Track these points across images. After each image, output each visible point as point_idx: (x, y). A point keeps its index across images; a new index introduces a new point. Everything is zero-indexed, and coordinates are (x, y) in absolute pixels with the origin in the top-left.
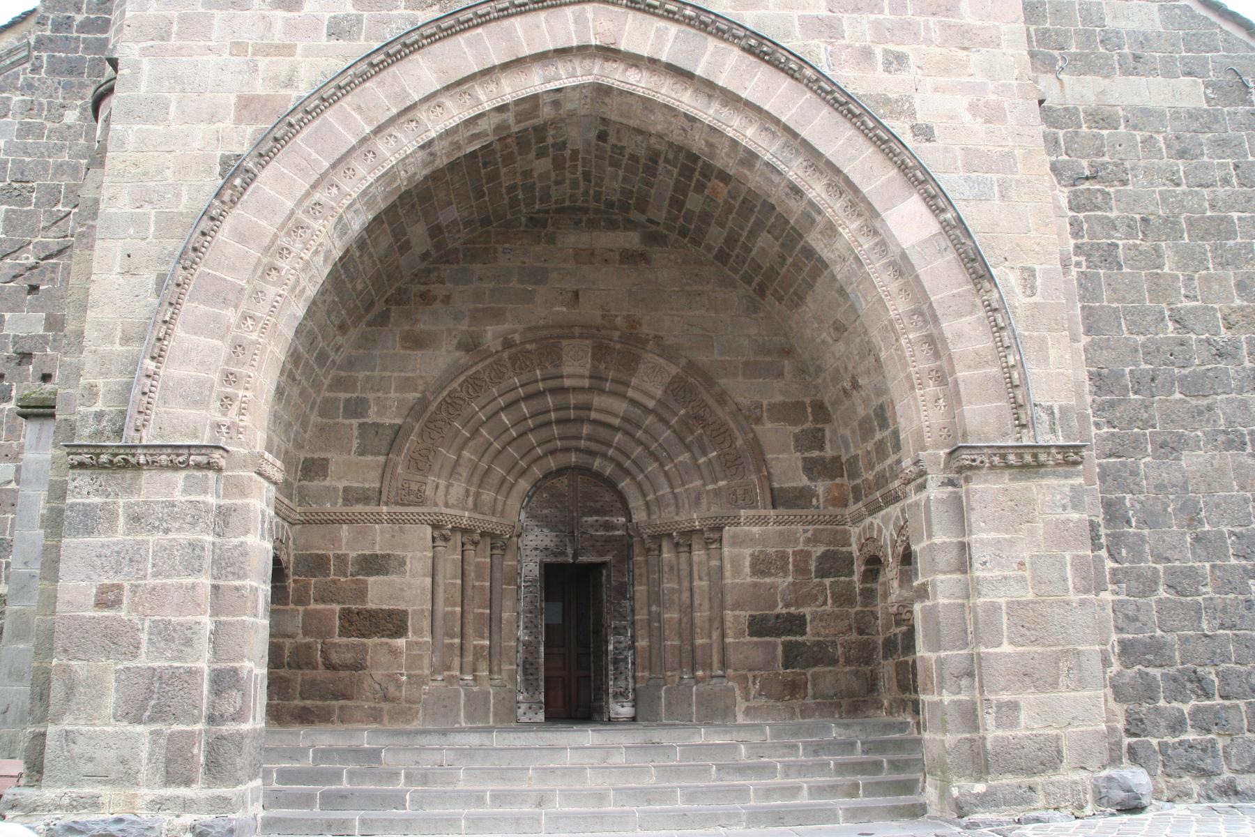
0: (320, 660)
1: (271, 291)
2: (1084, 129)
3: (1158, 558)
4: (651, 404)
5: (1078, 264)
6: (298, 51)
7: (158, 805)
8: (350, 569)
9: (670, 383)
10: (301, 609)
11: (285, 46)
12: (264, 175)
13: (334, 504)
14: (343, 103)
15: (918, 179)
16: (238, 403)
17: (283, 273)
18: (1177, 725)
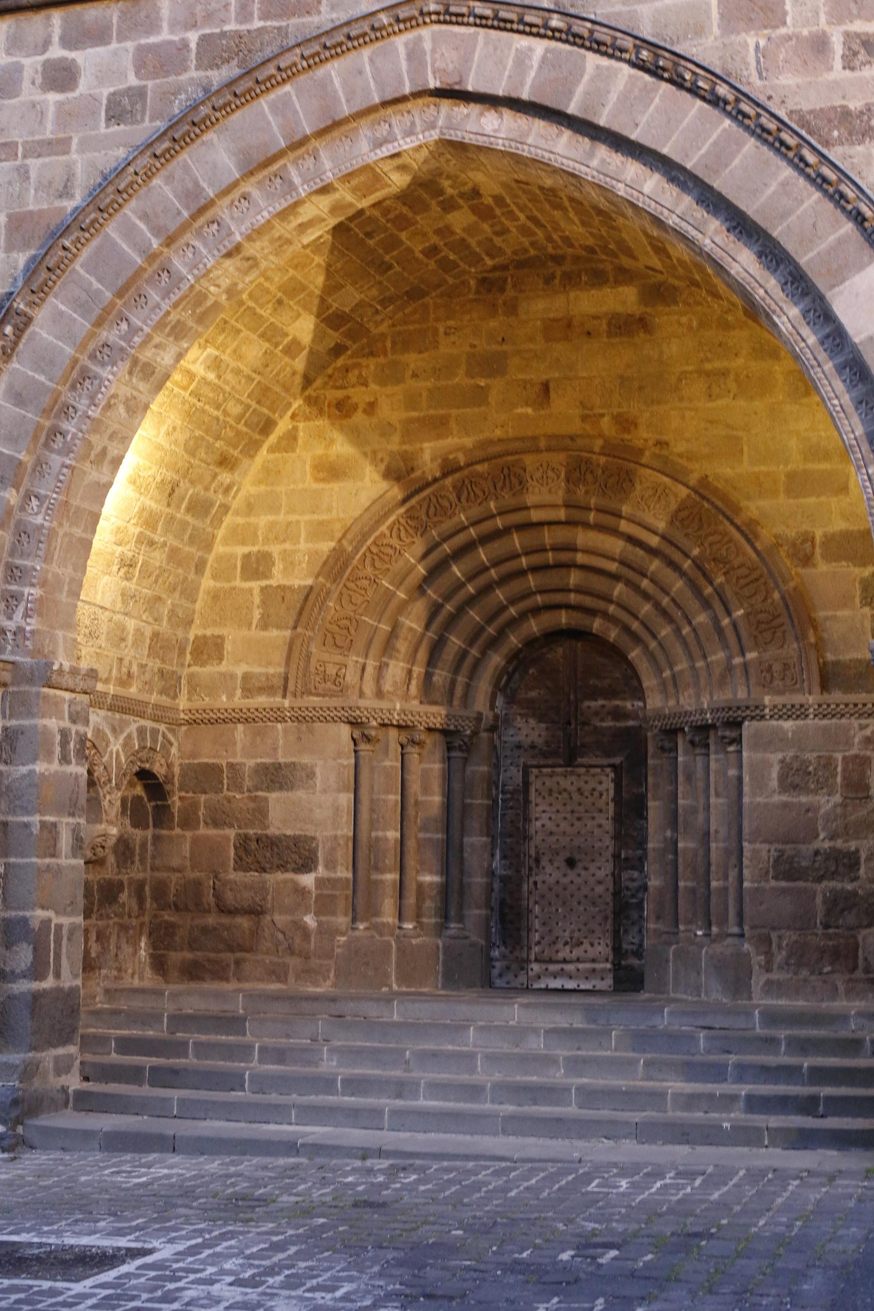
0: (212, 900)
1: (56, 460)
4: (654, 541)
6: (74, 145)
8: (247, 783)
9: (679, 510)
10: (189, 834)
11: (59, 141)
12: (41, 315)
13: (231, 696)
14: (127, 211)
16: (23, 604)
17: (69, 438)
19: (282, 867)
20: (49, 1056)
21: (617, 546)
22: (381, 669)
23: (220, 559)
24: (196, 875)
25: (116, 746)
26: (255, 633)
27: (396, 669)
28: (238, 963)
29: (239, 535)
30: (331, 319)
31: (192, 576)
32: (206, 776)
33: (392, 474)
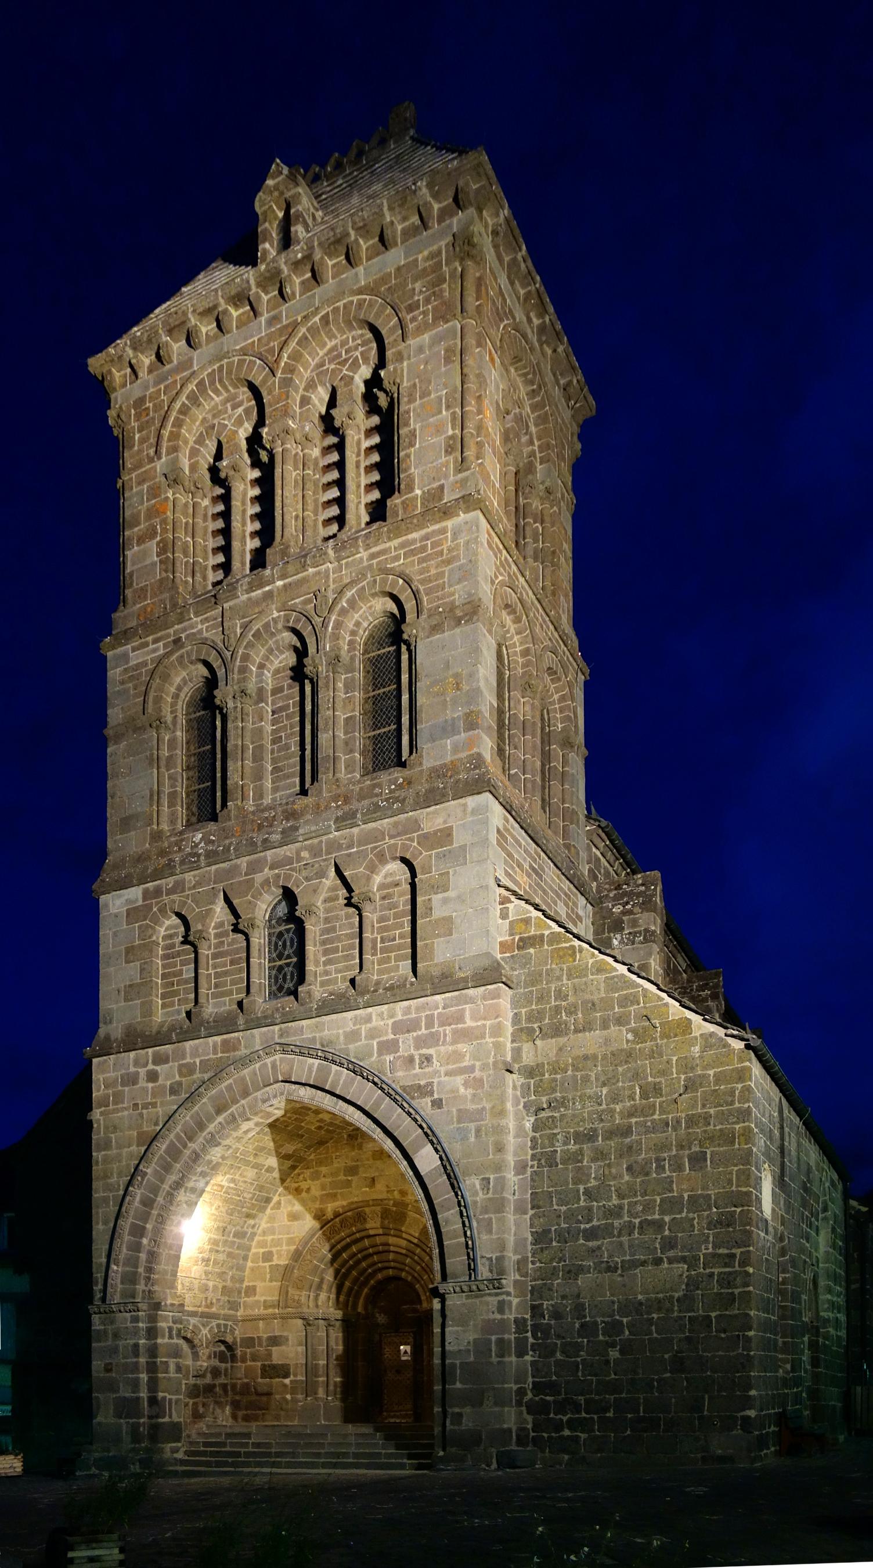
3: (558, 1337)
4: (416, 1241)
15: (430, 1136)
18: (559, 1427)
19: (278, 1377)
21: (404, 1243)
22: (318, 1295)
23: (254, 1254)
24: (246, 1381)
25: (205, 1331)
26: (268, 1284)
27: (323, 1296)
28: (263, 1414)
29: (262, 1244)
30: (283, 1157)
31: (241, 1262)
32: (249, 1342)
33: (317, 1217)
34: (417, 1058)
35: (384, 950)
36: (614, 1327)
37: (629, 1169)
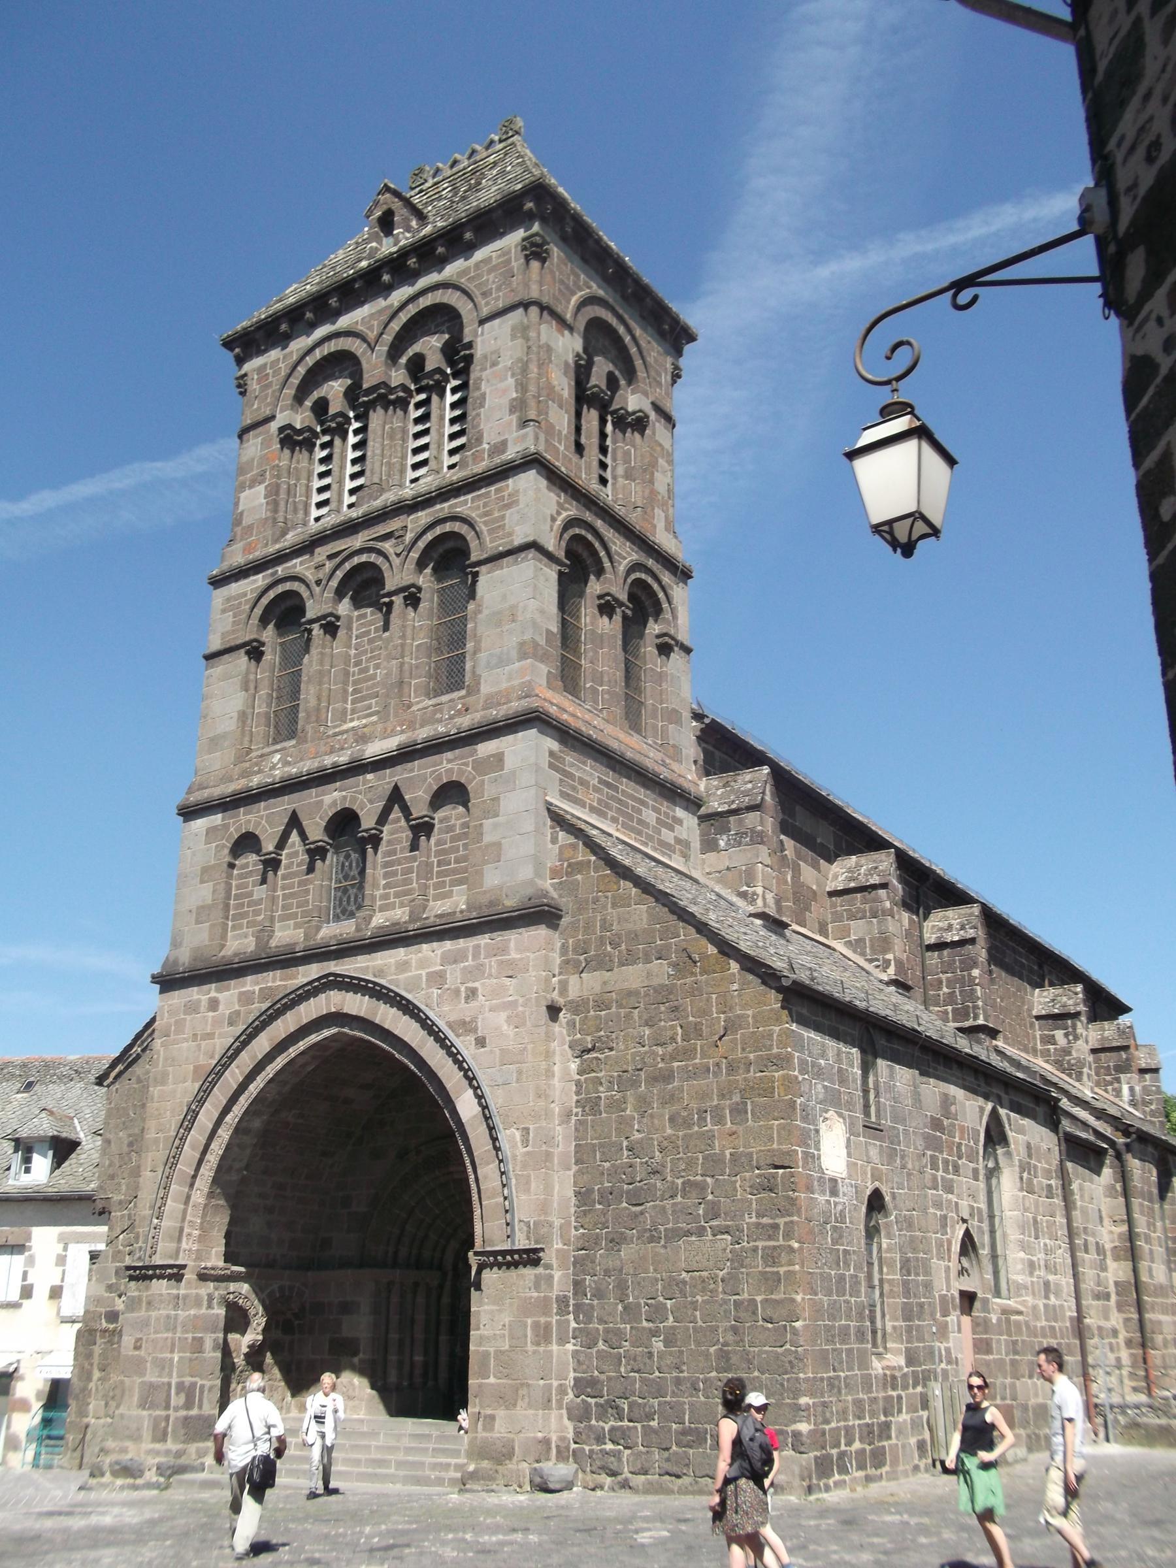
2: (592, 1013)
3: (601, 1321)
5: (576, 1115)
7: (149, 1452)
20: (193, 1448)
34: (463, 989)
35: (440, 874)
36: (657, 1313)
37: (672, 1119)
